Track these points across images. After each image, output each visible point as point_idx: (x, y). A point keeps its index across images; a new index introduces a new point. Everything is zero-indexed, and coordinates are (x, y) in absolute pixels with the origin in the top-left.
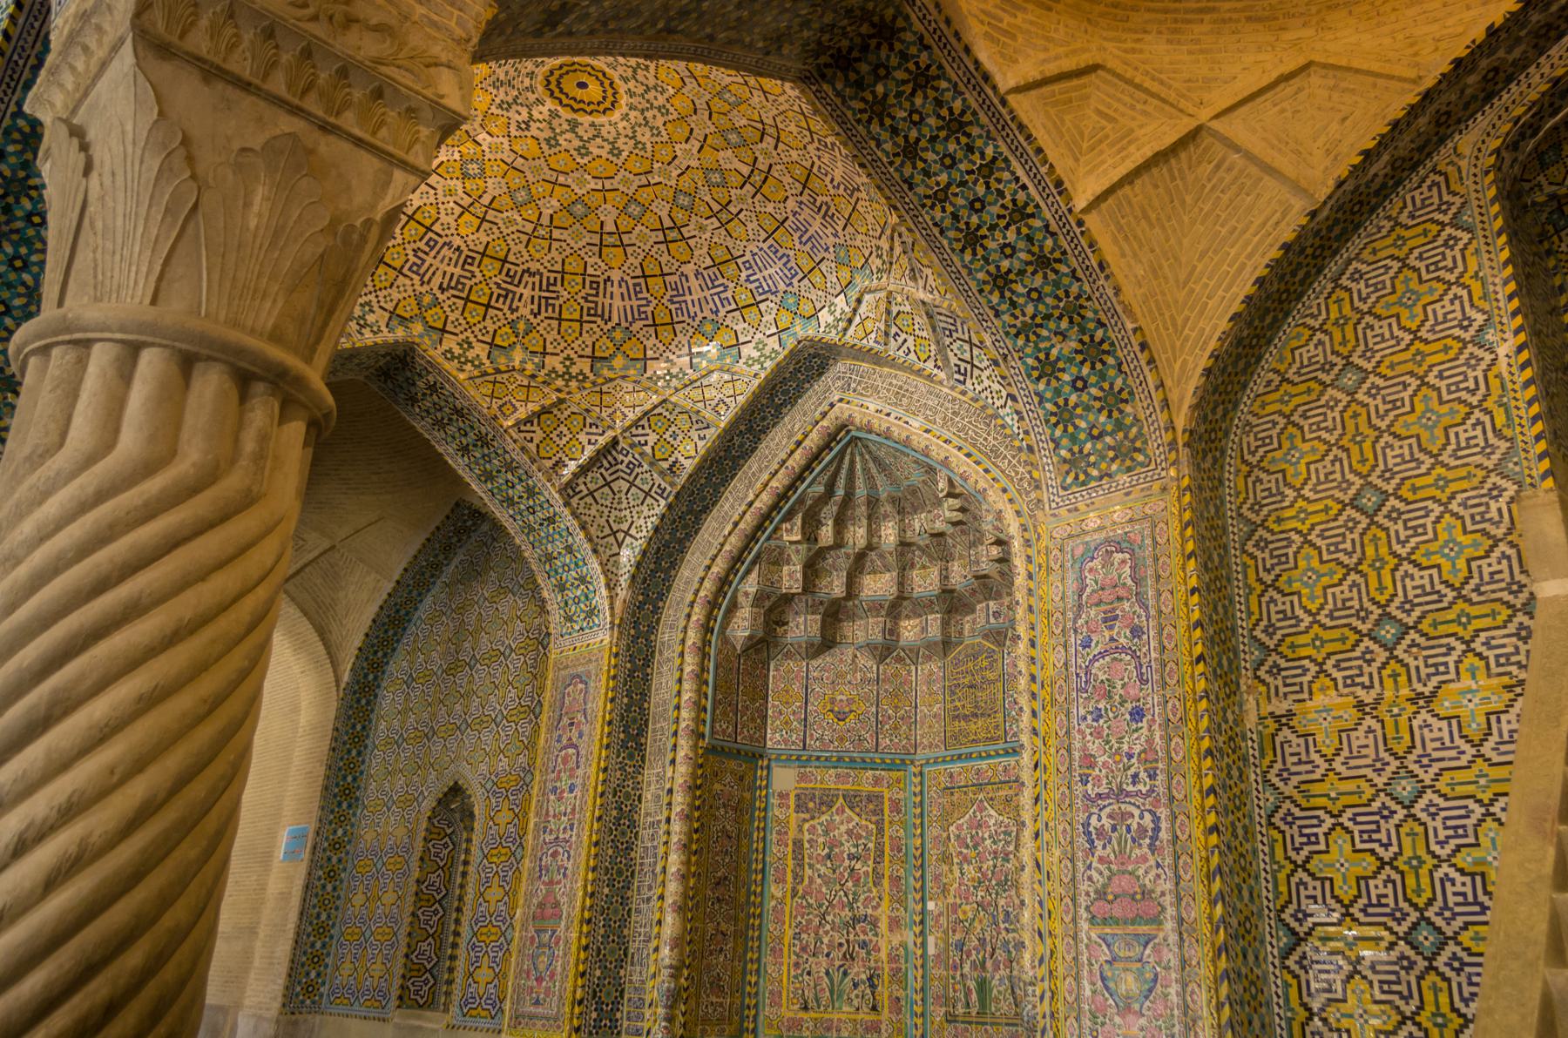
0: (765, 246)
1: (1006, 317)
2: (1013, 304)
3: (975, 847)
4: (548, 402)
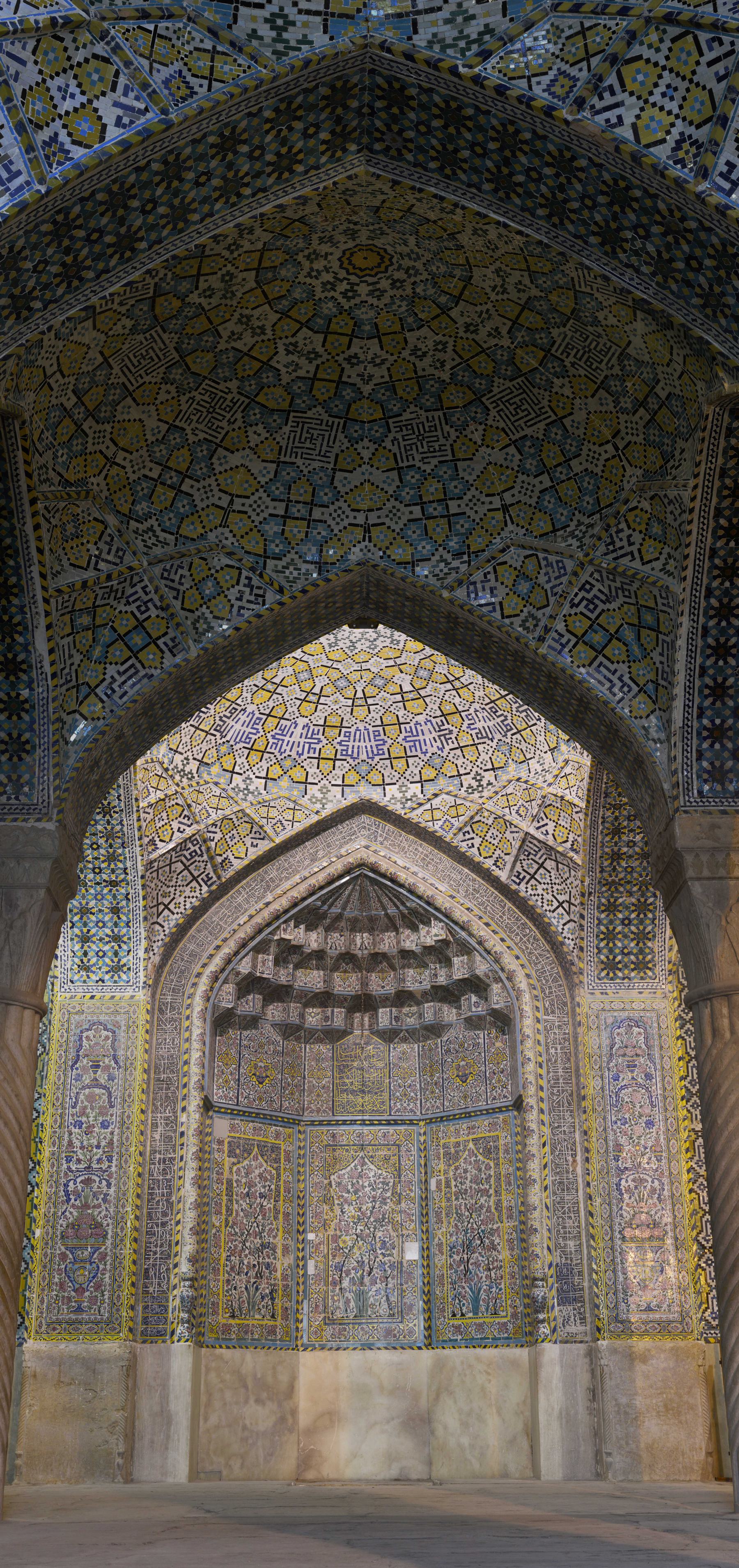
0: (371, 729)
1: (605, 875)
2: (614, 869)
3: (356, 1192)
4: (170, 793)
